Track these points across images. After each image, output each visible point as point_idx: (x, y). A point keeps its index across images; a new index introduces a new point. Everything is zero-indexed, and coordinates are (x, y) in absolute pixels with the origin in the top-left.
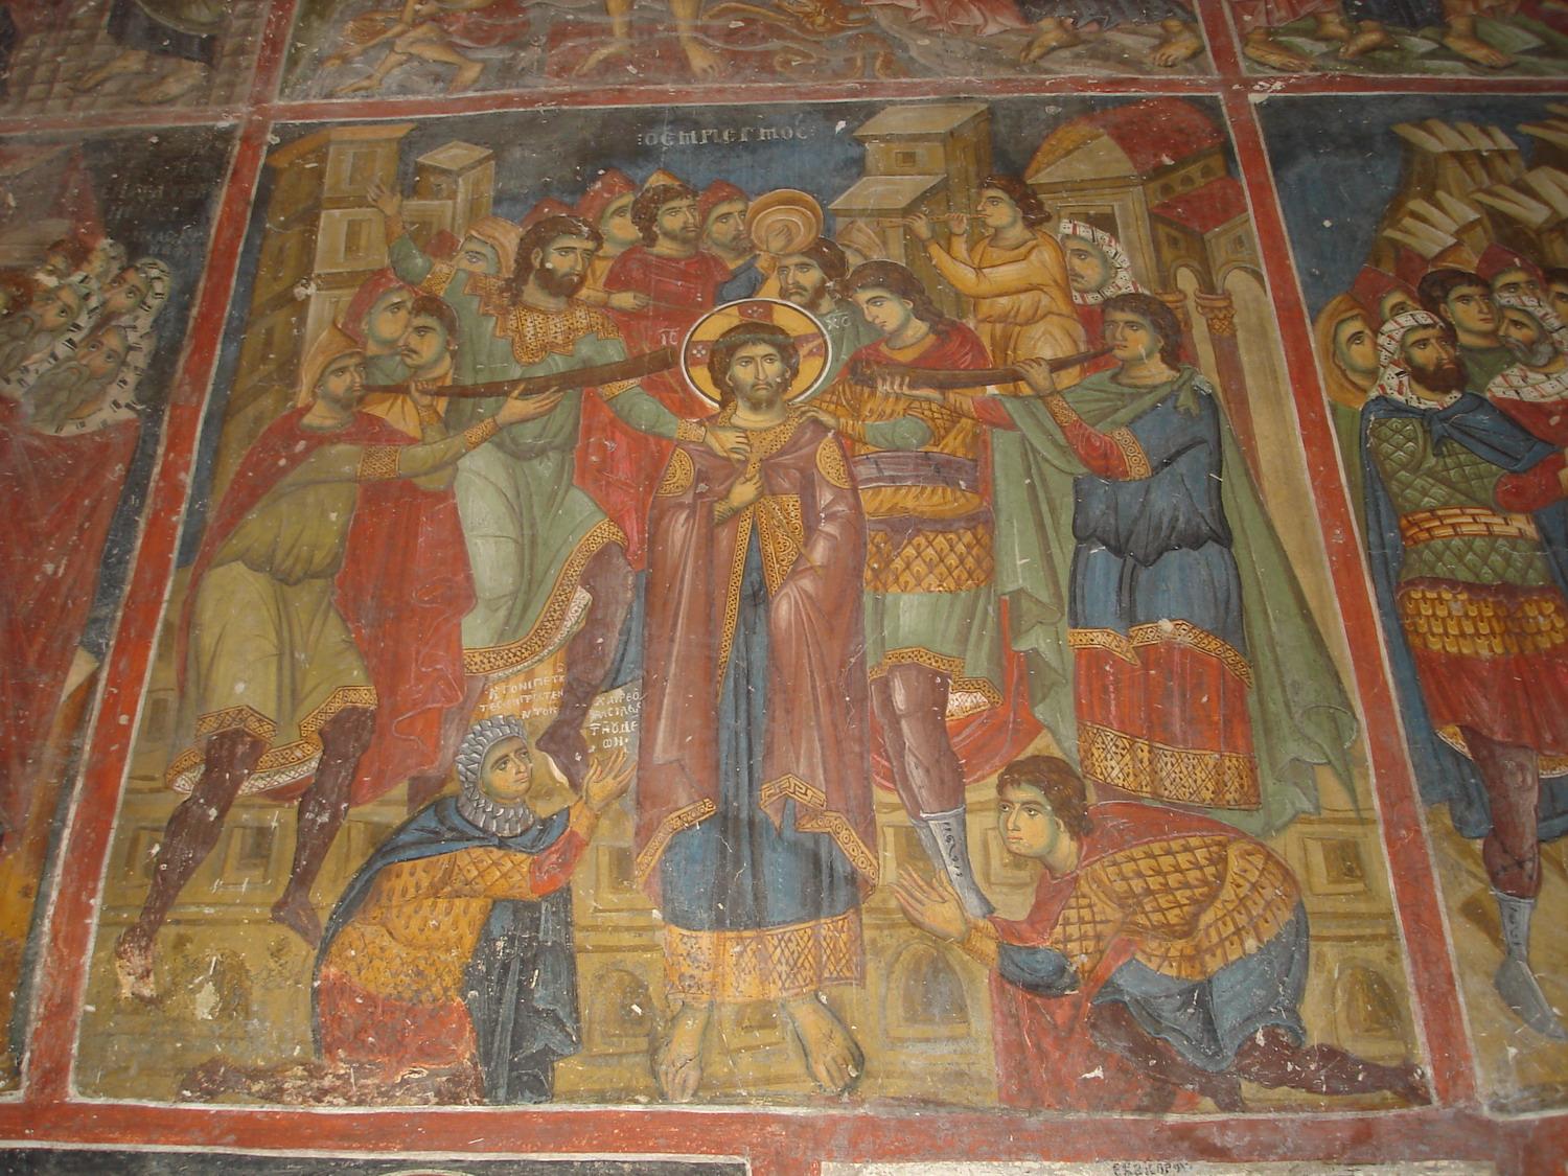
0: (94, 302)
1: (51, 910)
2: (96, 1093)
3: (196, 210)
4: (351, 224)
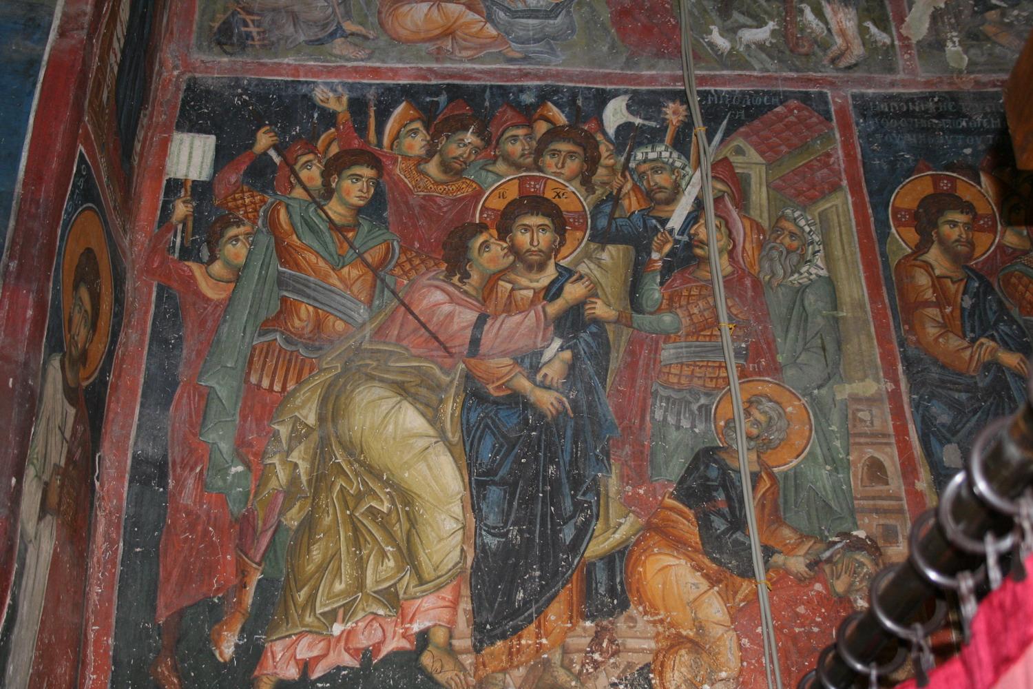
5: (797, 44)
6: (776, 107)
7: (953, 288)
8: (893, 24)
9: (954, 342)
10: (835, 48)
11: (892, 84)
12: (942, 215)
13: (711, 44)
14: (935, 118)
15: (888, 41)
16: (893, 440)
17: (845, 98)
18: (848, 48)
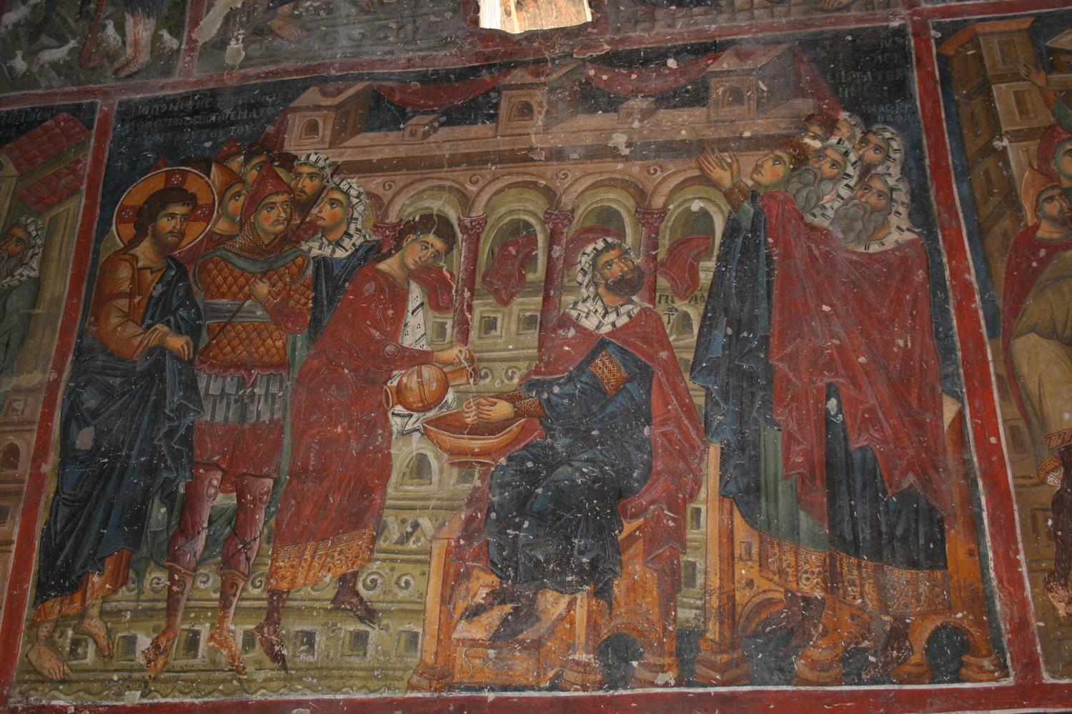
0: (853, 157)
1: (992, 564)
2: (1062, 677)
3: (900, 89)
4: (1016, 93)
5: (89, 59)
6: (45, 120)
7: (148, 276)
8: (187, 29)
9: (132, 329)
10: (122, 59)
11: (162, 88)
12: (165, 209)
13: (11, 69)
14: (189, 116)
15: (175, 47)
16: (36, 427)
17: (111, 106)
18: (135, 57)
